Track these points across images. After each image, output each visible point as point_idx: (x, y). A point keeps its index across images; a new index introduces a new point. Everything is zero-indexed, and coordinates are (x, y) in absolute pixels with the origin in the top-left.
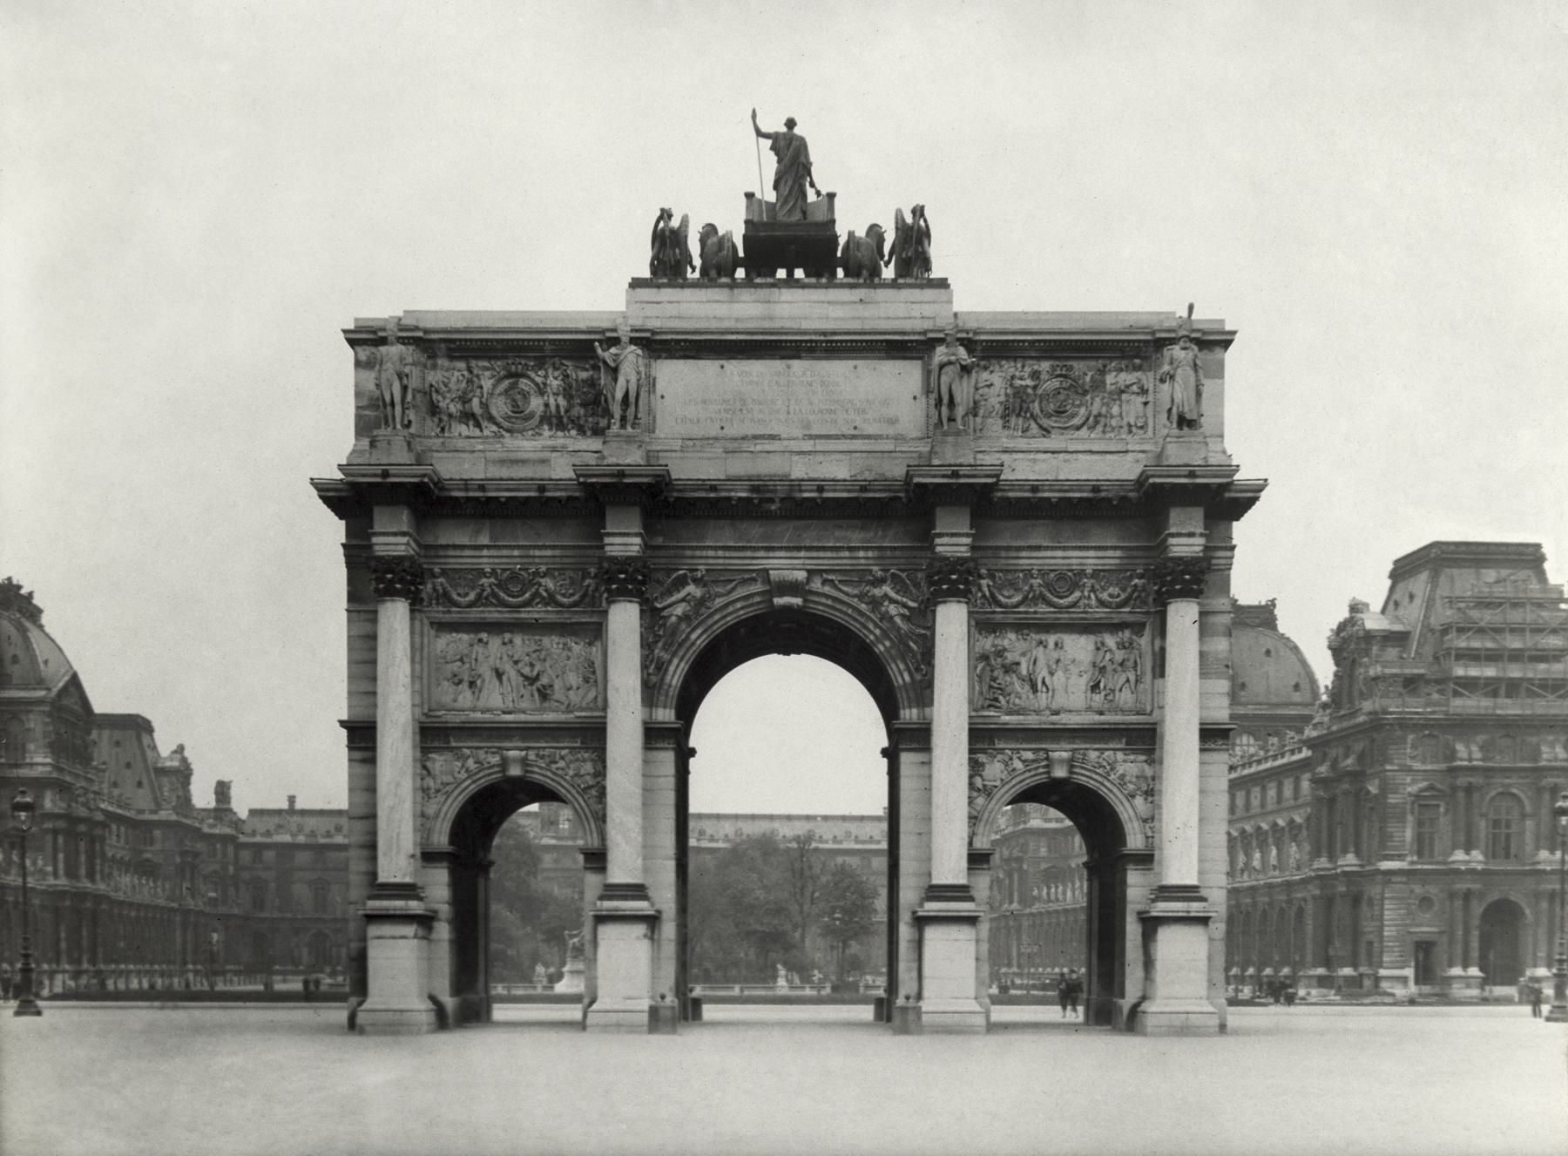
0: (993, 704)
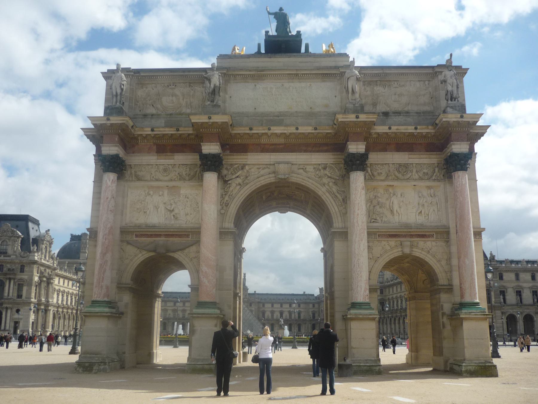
0: (375, 221)
